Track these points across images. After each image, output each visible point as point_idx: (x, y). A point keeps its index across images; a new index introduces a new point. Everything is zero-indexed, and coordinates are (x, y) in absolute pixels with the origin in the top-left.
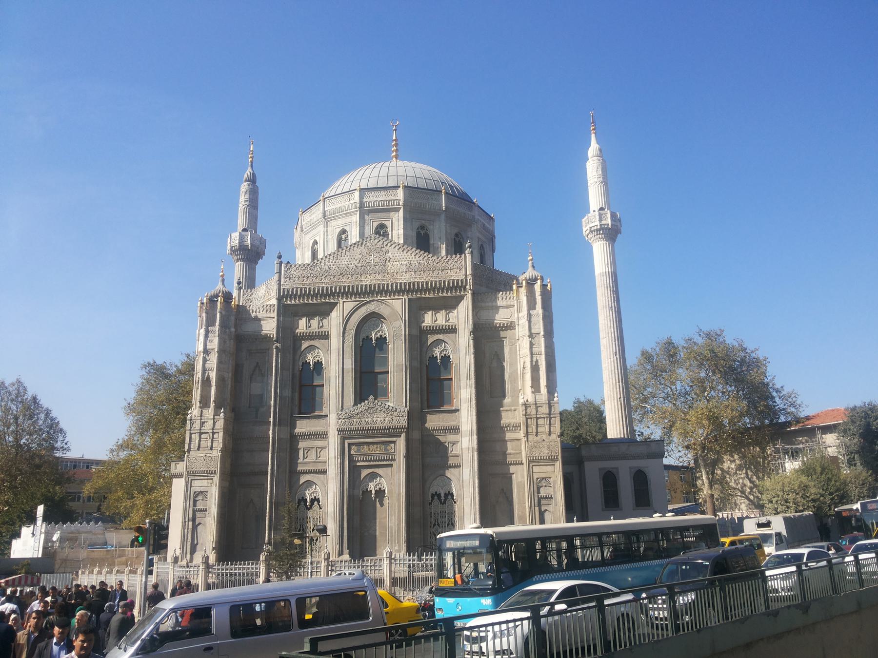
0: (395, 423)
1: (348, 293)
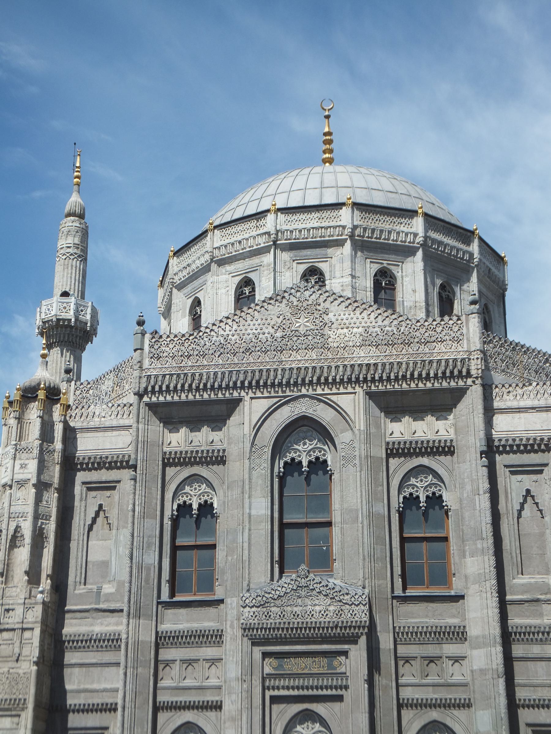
0: (346, 617)
1: (258, 384)
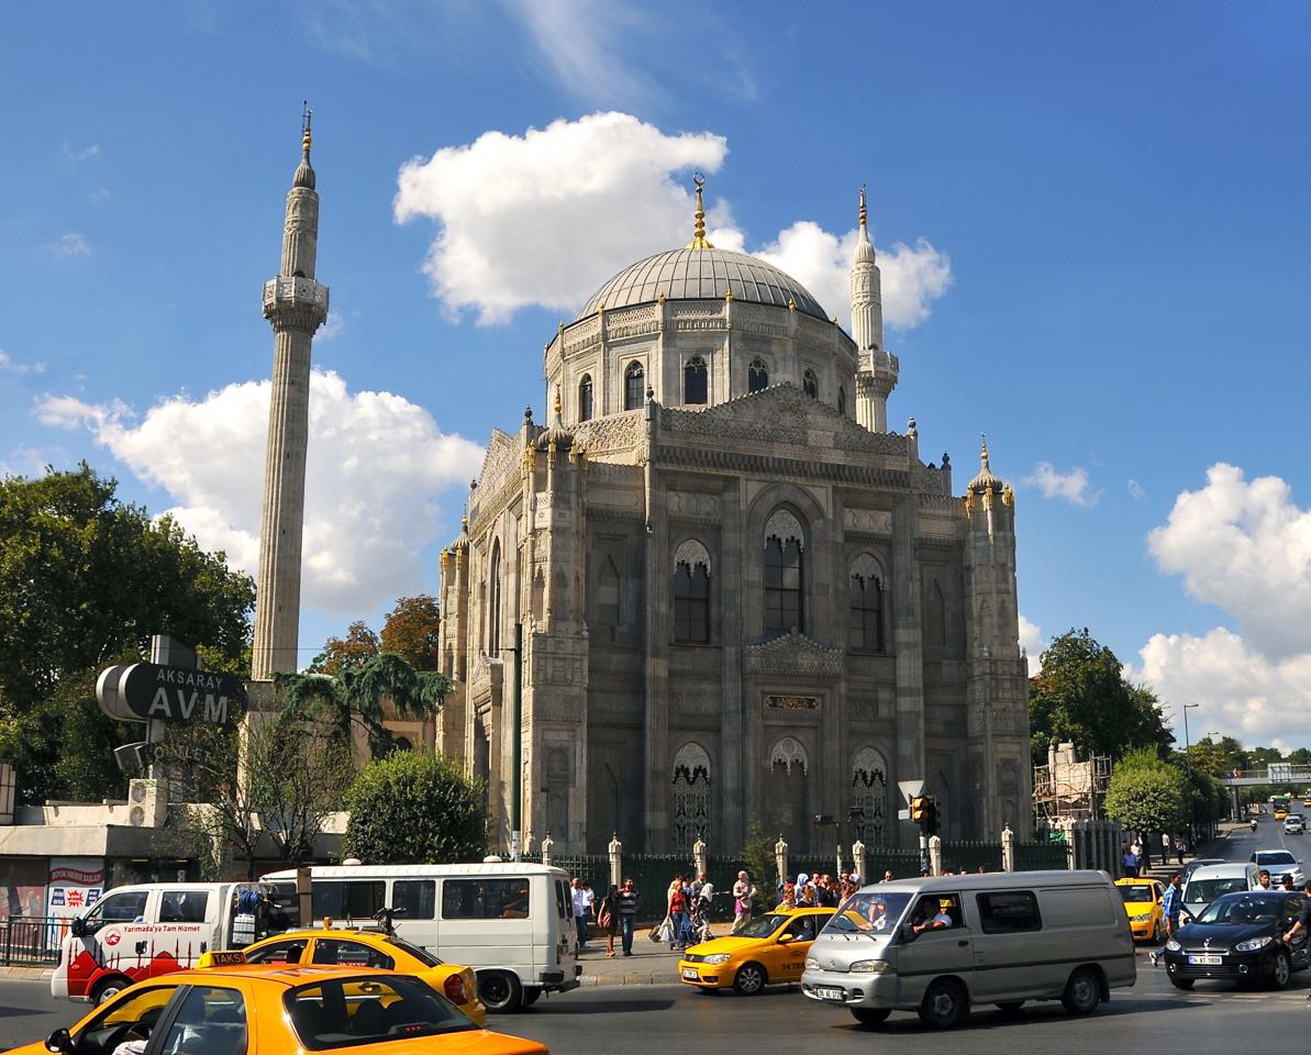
1: (755, 465)
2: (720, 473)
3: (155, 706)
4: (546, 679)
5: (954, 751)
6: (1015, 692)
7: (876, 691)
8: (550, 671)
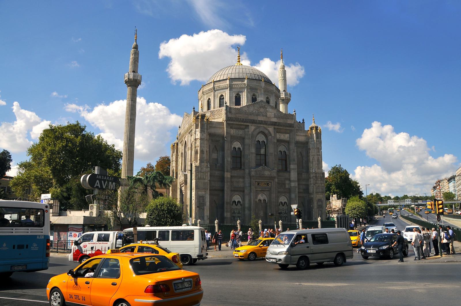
1: (253, 122)
2: (244, 124)
3: (96, 185)
4: (199, 178)
5: (305, 197)
6: (321, 181)
7: (285, 181)
8: (199, 176)
